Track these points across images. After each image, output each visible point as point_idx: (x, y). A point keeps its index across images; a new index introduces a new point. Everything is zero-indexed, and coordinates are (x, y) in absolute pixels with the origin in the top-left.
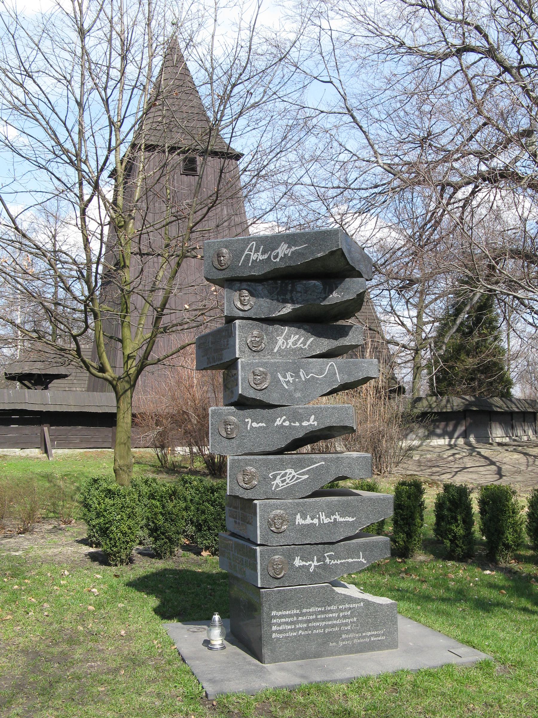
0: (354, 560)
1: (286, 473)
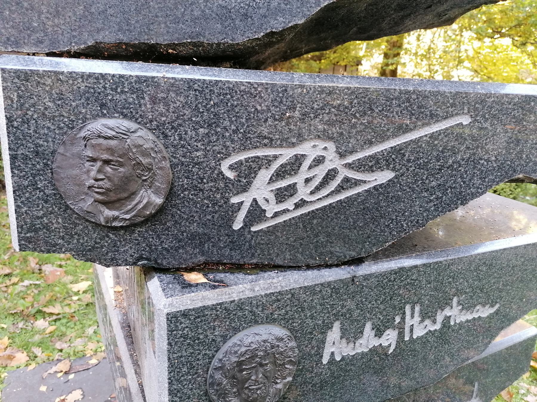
1: (298, 160)
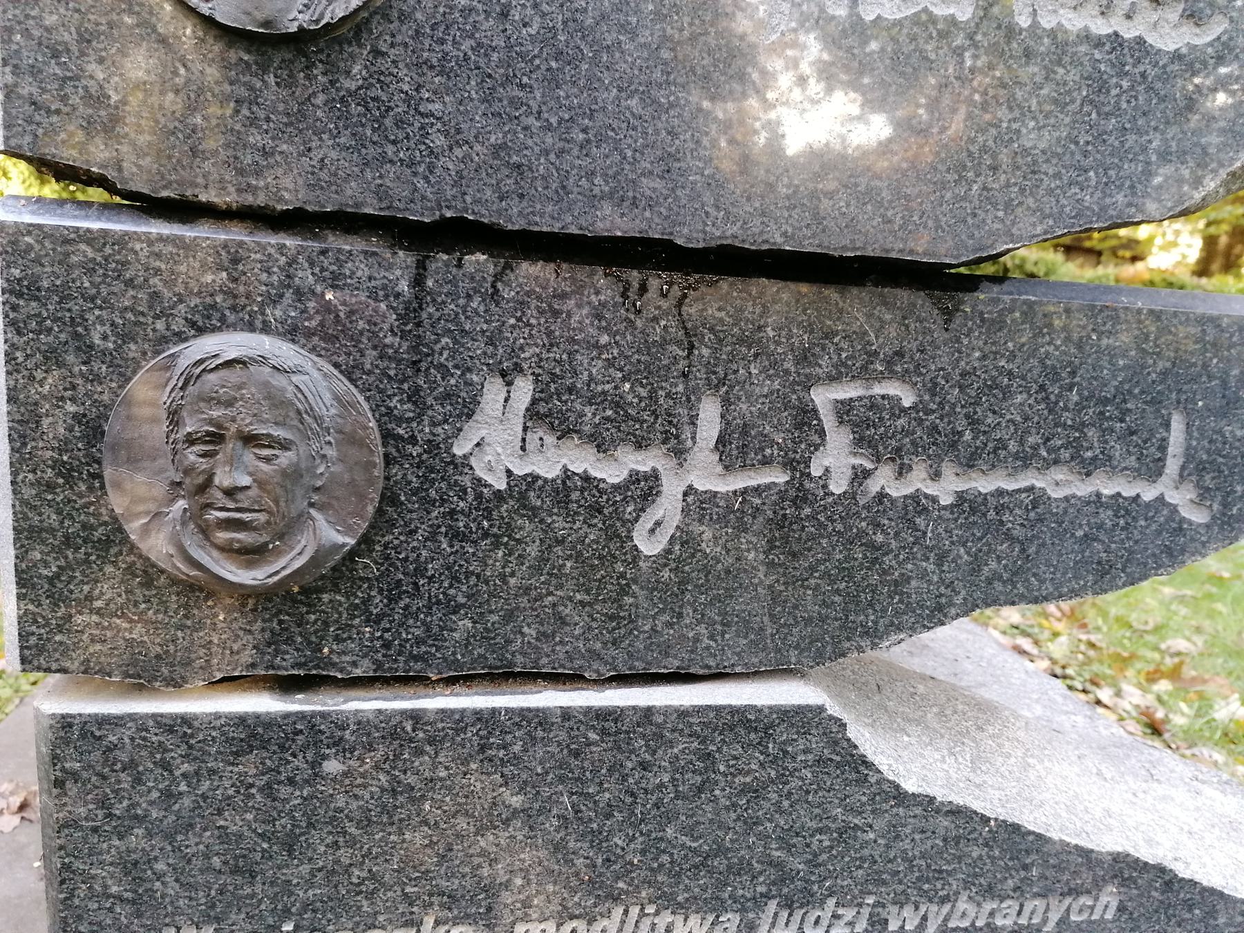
0: (1108, 486)
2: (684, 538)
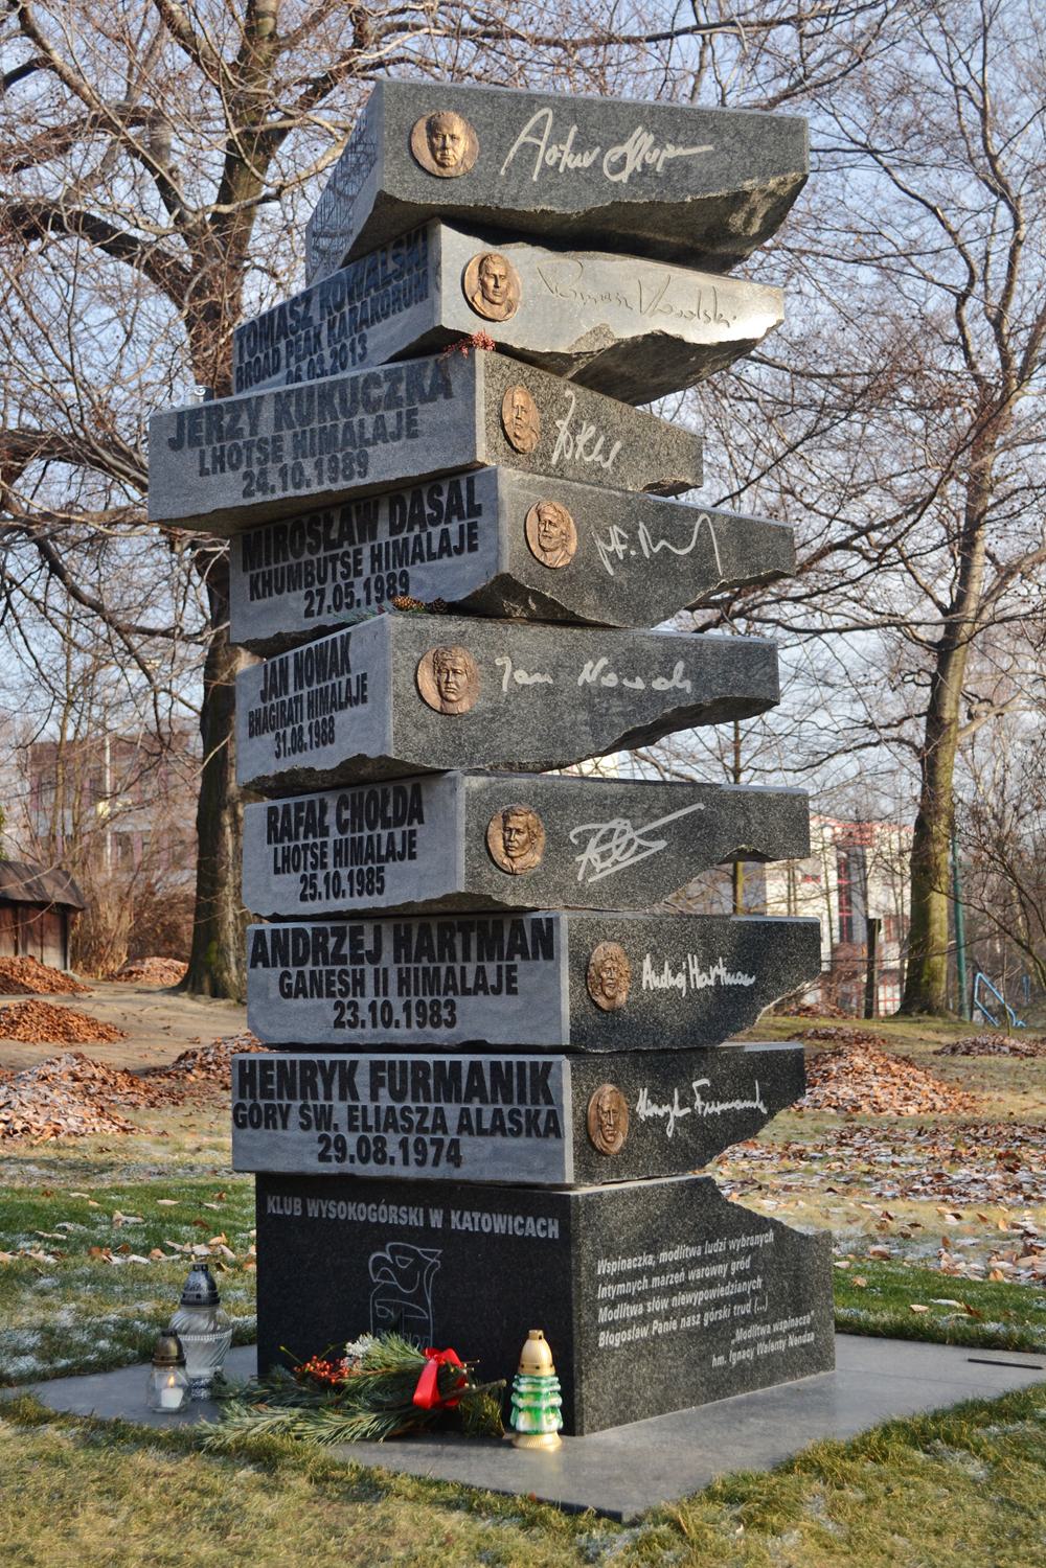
1: (612, 831)
2: (675, 1132)
